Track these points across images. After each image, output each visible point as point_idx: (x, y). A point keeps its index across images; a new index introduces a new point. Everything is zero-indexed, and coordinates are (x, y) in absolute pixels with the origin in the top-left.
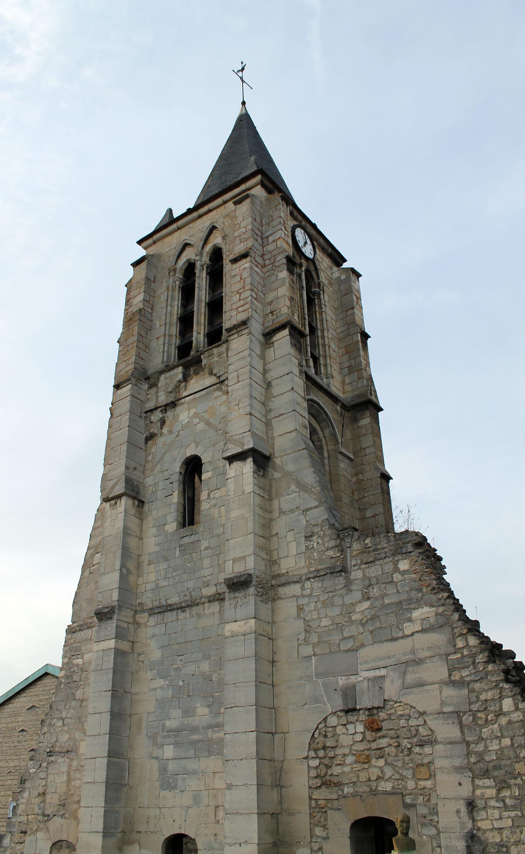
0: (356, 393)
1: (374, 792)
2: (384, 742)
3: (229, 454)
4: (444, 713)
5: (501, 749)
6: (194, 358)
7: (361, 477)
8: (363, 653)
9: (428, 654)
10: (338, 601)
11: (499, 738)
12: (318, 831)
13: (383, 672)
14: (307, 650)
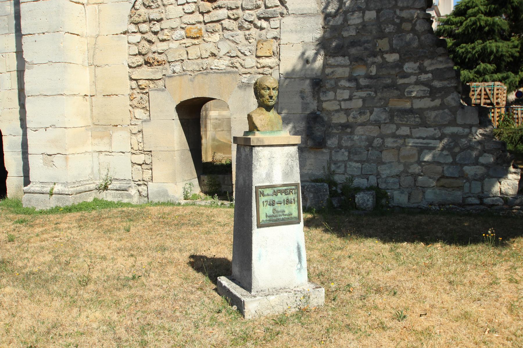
1: (205, 71)
5: (364, 25)
11: (363, 11)
12: (139, 113)
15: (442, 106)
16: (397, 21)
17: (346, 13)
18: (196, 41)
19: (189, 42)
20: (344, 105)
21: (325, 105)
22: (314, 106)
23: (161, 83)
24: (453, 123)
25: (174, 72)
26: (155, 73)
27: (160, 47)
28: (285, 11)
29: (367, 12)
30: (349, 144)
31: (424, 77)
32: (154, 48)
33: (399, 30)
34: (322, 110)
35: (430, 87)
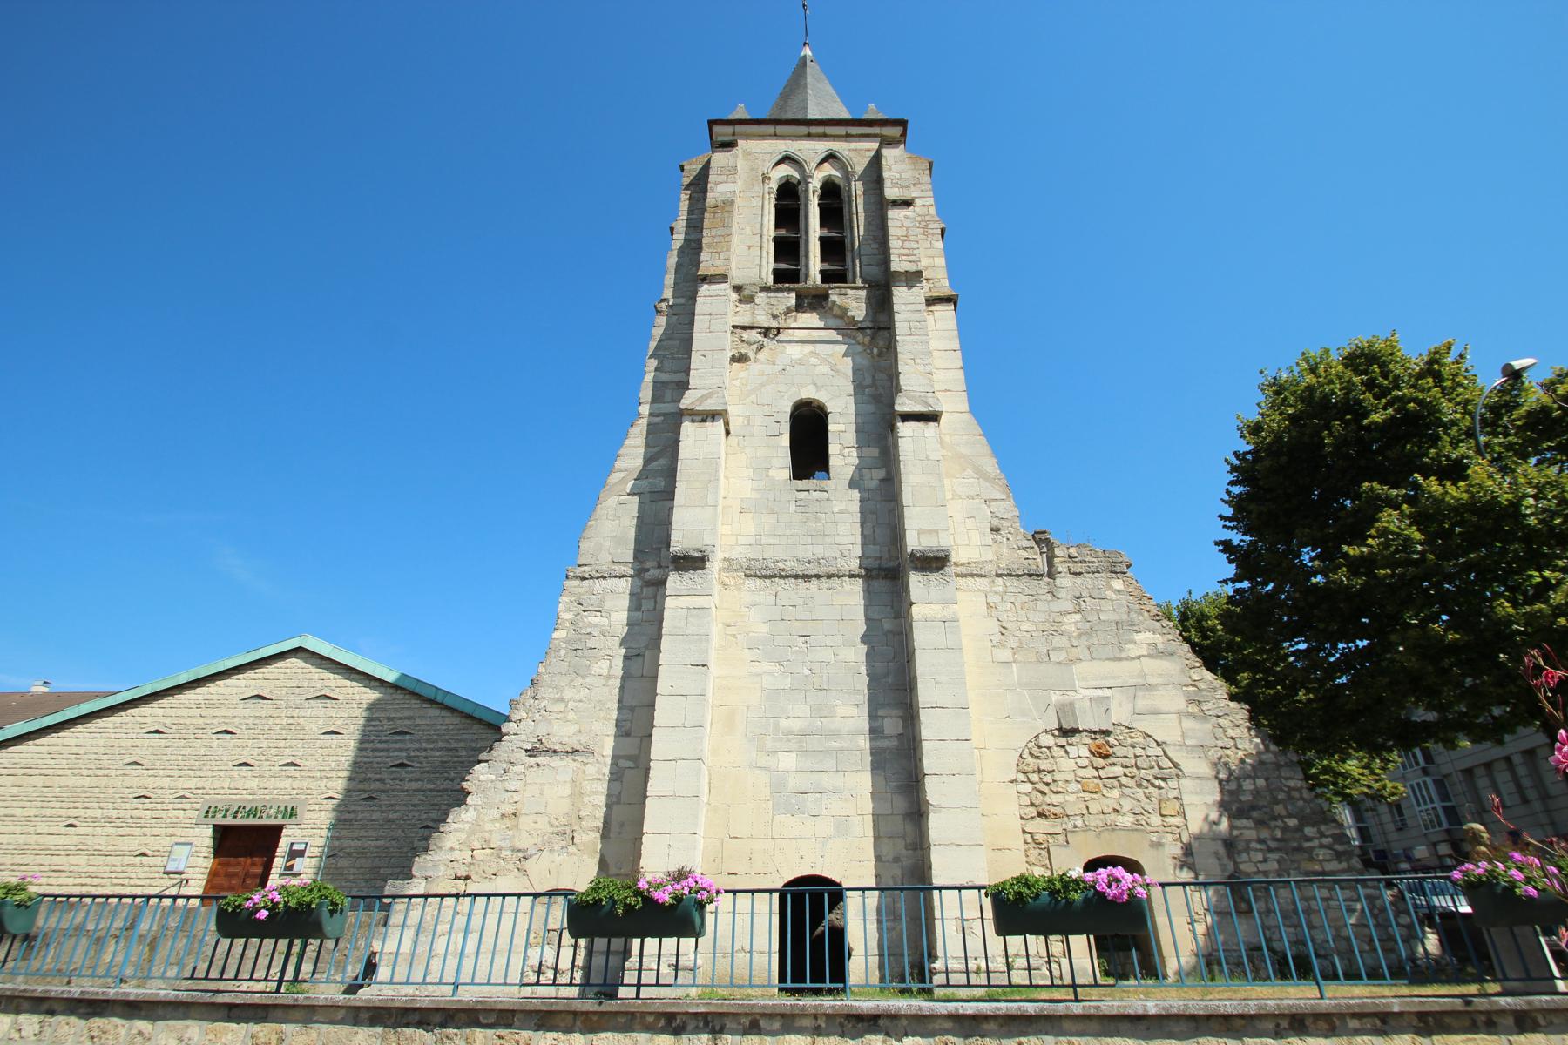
1: (1113, 827)
2: (1118, 770)
4: (1187, 746)
8: (1077, 669)
9: (1160, 681)
13: (1107, 693)
14: (1005, 654)
16: (1286, 789)
17: (1238, 779)
18: (1094, 796)
19: (1087, 796)
21: (1242, 867)
22: (1231, 867)
25: (1075, 827)
26: (1053, 826)
27: (1056, 799)
29: (1257, 780)
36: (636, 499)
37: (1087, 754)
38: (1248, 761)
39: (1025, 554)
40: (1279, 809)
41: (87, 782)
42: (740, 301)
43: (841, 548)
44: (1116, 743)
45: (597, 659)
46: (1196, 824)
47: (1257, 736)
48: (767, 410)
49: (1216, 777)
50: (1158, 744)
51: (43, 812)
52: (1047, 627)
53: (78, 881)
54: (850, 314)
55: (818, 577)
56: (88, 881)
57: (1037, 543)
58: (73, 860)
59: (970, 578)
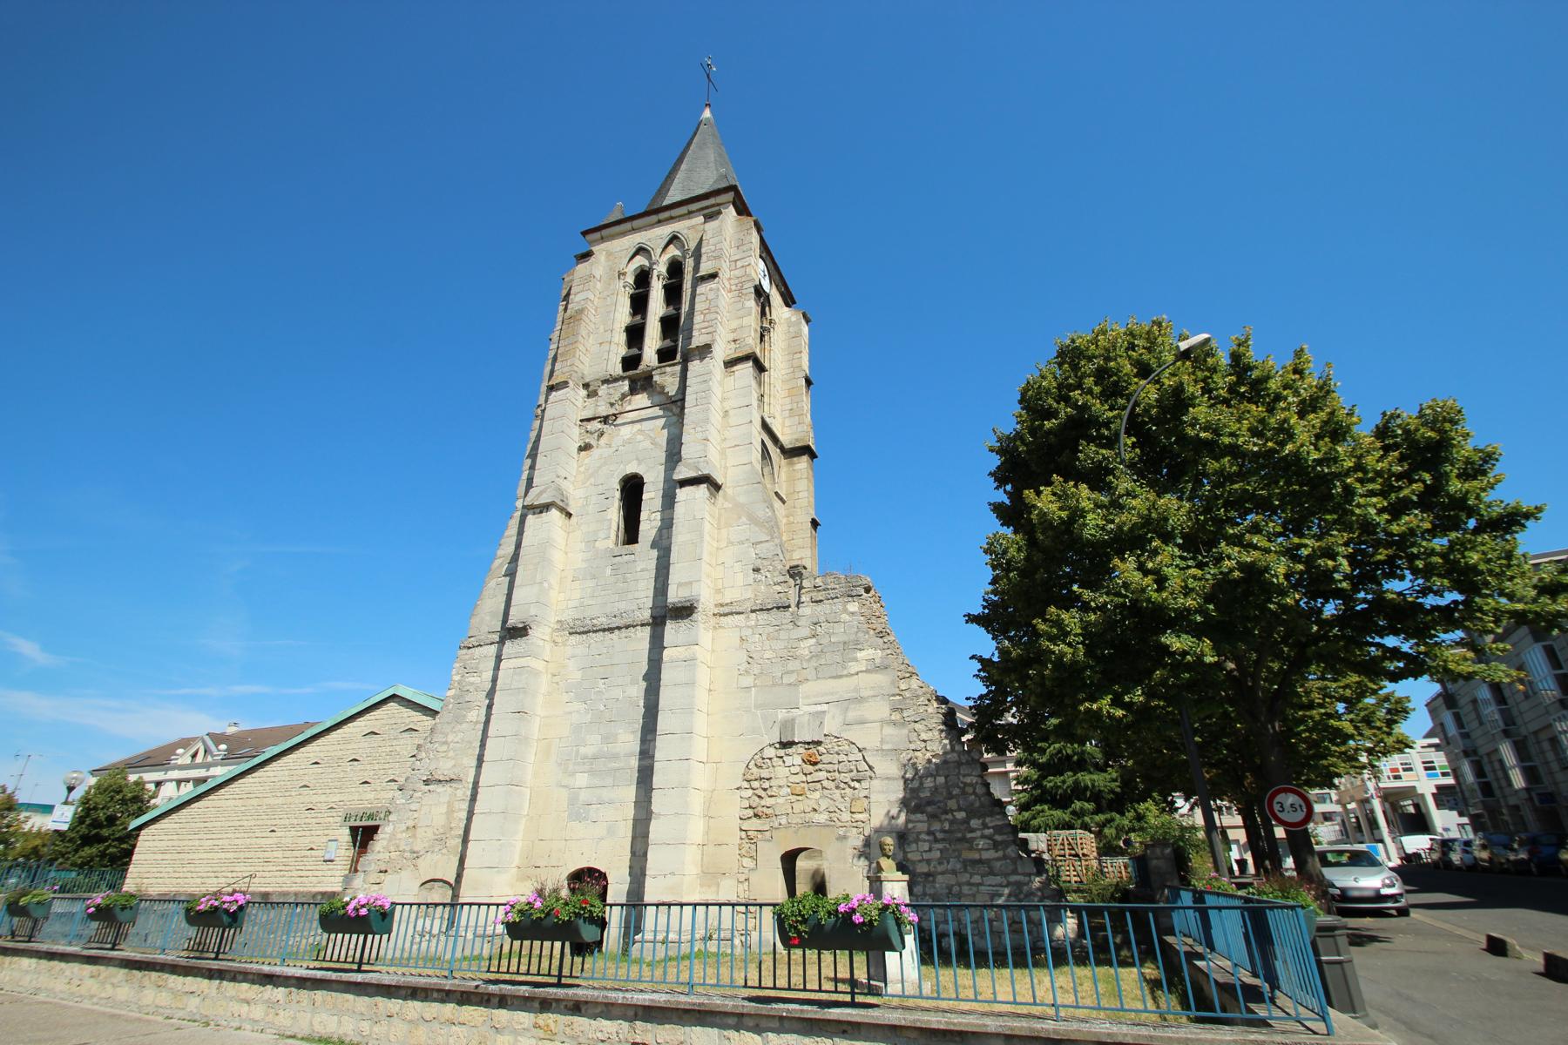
0: (795, 436)
1: (808, 824)
2: (822, 775)
3: (681, 477)
5: (936, 788)
6: (644, 372)
7: (791, 519)
8: (803, 688)
9: (872, 693)
10: (783, 635)
12: (747, 862)
14: (748, 681)
15: (1005, 857)
17: (921, 777)
18: (800, 798)
20: (926, 856)
21: (909, 856)
23: (768, 834)
24: (1015, 872)
27: (768, 801)
28: (873, 775)
29: (938, 778)
30: (932, 891)
31: (988, 832)
32: (763, 803)
33: (964, 793)
34: (908, 860)
35: (993, 840)
36: (508, 578)
37: (800, 762)
38: (934, 760)
39: (778, 588)
40: (952, 804)
41: (280, 800)
42: (589, 396)
43: (638, 601)
44: (825, 751)
45: (470, 709)
46: (878, 819)
47: (946, 738)
48: (600, 489)
49: (903, 777)
50: (860, 750)
51: (258, 823)
52: (785, 653)
53: (278, 868)
54: (666, 390)
55: (619, 628)
56: (283, 868)
57: (791, 576)
58: (275, 854)
59: (730, 617)
